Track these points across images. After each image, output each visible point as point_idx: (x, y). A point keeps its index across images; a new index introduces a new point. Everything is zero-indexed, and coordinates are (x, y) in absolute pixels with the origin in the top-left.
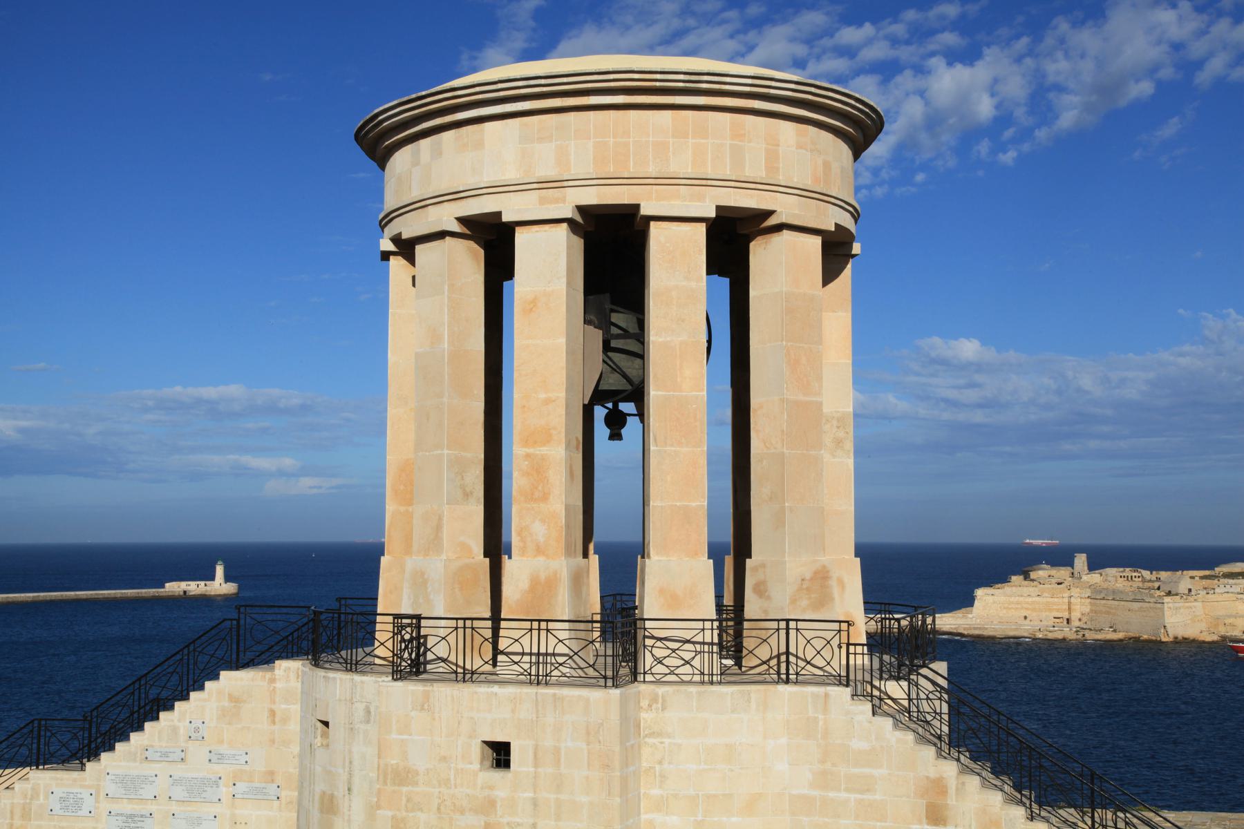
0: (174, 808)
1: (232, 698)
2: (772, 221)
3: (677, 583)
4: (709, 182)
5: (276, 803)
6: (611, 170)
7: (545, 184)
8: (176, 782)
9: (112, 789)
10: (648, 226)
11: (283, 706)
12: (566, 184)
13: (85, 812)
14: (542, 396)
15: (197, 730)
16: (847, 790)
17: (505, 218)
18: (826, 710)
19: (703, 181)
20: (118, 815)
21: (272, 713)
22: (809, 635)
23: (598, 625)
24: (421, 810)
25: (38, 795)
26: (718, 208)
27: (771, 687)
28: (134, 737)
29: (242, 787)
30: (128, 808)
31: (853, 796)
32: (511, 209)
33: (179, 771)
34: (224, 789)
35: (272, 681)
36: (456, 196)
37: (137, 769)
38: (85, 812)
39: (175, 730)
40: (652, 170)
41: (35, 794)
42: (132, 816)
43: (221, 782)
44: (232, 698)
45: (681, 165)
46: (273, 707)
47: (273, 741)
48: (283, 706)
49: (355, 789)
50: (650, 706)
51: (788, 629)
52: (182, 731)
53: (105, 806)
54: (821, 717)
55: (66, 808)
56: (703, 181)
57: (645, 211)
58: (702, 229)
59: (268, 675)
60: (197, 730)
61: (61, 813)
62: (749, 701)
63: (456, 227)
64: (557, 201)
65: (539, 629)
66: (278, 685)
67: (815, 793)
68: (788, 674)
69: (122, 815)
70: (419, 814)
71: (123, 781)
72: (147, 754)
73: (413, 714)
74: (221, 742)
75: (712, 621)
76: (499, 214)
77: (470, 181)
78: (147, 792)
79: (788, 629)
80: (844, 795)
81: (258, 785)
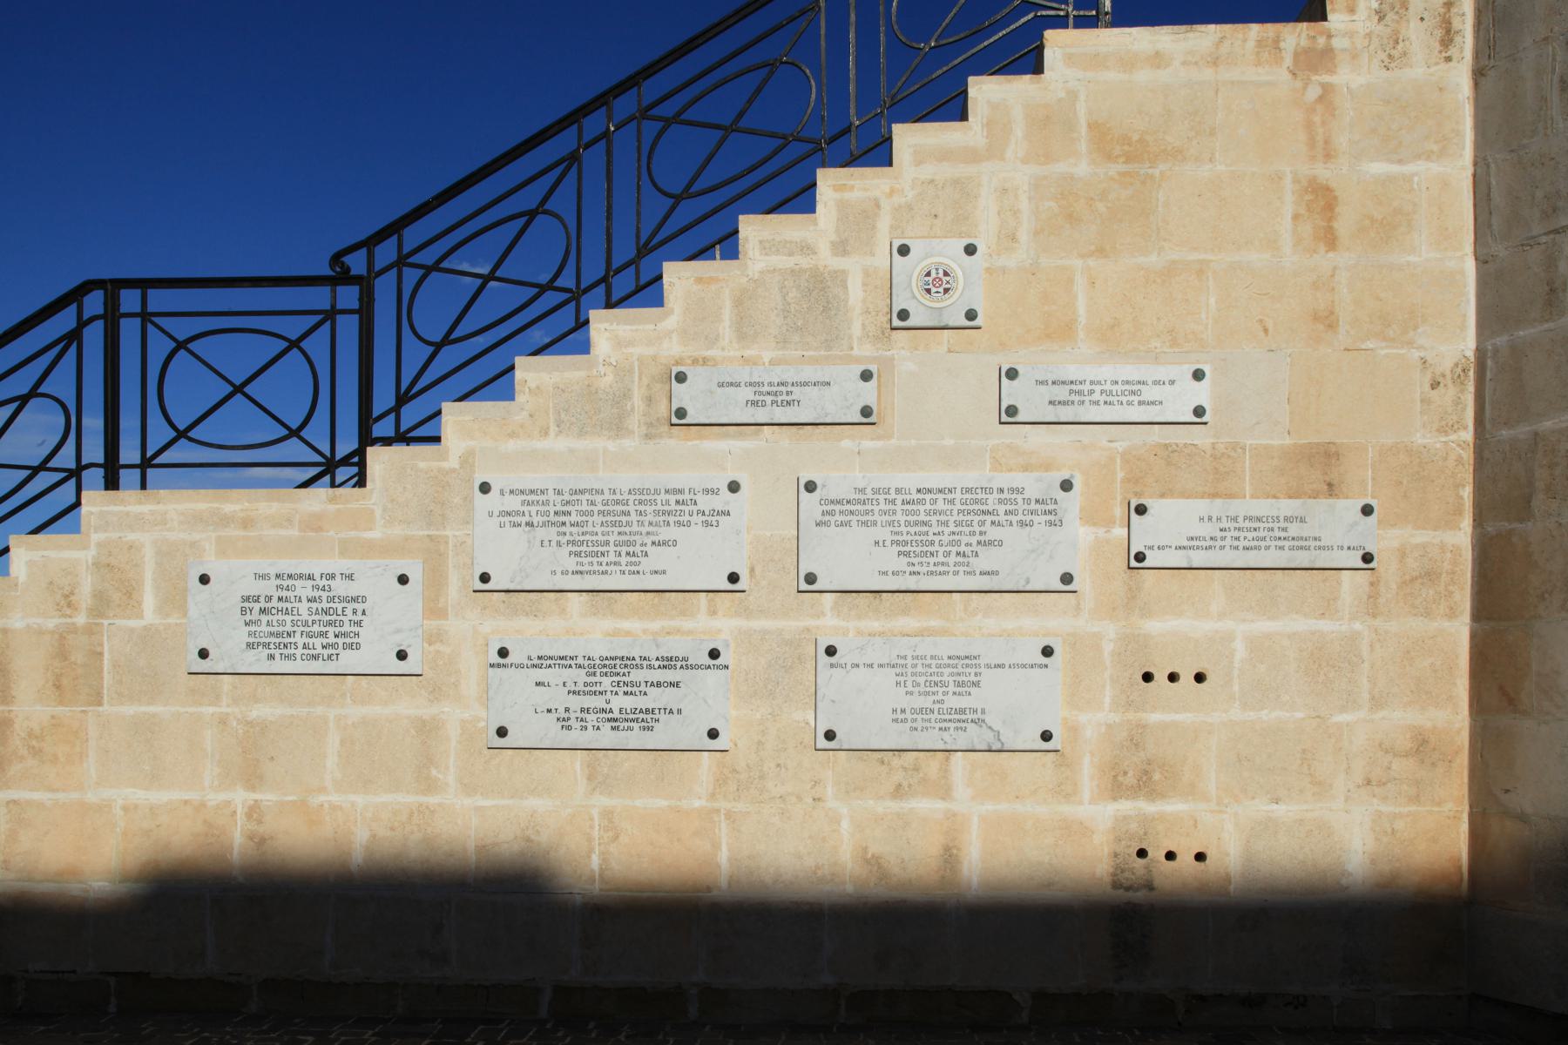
0: (829, 621)
1: (1105, 141)
5: (1351, 585)
8: (849, 510)
9: (508, 553)
11: (1378, 168)
13: (374, 653)
15: (938, 282)
20: (542, 661)
21: (1322, 201)
25: (130, 593)
28: (608, 328)
29: (1173, 523)
30: (594, 632)
33: (845, 466)
34: (1084, 534)
35: (1317, 60)
37: (629, 463)
38: (374, 653)
39: (820, 291)
41: (116, 589)
43: (1070, 504)
44: (1100, 132)
46: (1323, 172)
47: (1327, 320)
48: (1378, 168)
52: (855, 292)
53: (475, 628)
55: (281, 643)
59: (1294, 35)
60: (938, 282)
61: (256, 661)
66: (1345, 77)
69: (564, 661)
71: (557, 514)
72: (683, 395)
74: (1060, 331)
78: (694, 558)
81: (1262, 507)
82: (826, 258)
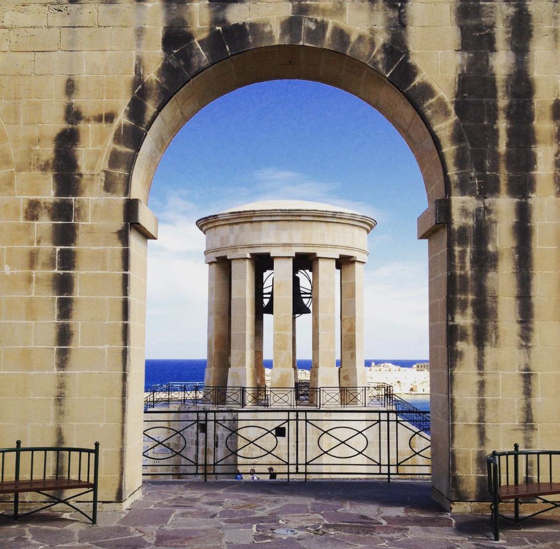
2: (352, 259)
6: (307, 242)
7: (285, 245)
10: (318, 260)
12: (292, 245)
14: (284, 315)
17: (272, 255)
19: (335, 247)
22: (289, 395)
24: (254, 450)
26: (340, 255)
36: (251, 247)
40: (320, 242)
45: (328, 241)
51: (365, 390)
56: (335, 247)
57: (318, 255)
58: (334, 263)
63: (249, 256)
64: (289, 250)
68: (365, 404)
70: (253, 452)
77: (256, 242)
79: (365, 390)
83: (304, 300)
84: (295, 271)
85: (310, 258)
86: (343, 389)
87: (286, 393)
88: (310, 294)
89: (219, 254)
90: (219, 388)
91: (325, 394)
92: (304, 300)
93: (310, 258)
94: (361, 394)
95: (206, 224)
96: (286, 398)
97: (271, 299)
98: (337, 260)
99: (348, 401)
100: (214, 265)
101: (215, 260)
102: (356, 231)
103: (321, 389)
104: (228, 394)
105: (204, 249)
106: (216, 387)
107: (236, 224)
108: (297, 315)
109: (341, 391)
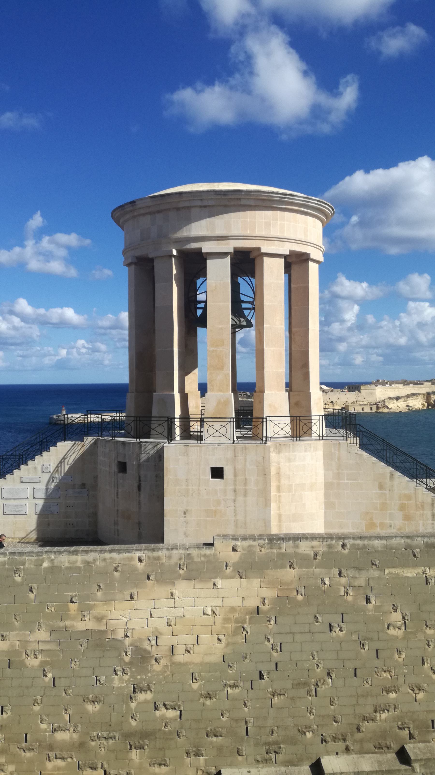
3: (275, 402)
4: (286, 240)
14: (220, 326)
16: (347, 479)
18: (339, 450)
19: (283, 240)
23: (199, 419)
26: (290, 251)
27: (318, 442)
31: (349, 482)
32: (207, 247)
40: (264, 233)
42: (16, 506)
49: (142, 489)
50: (274, 450)
54: (337, 452)
57: (263, 251)
62: (311, 447)
65: (296, 420)
67: (335, 481)
73: (180, 457)
75: (233, 418)
76: (201, 249)
80: (346, 481)
82: (36, 466)
83: (245, 311)
84: (234, 276)
85: (252, 256)
86: (295, 418)
87: (224, 424)
88: (252, 303)
89: (138, 253)
90: (141, 419)
91: (272, 425)
92: (245, 311)
93: (252, 256)
94: (318, 424)
95: (123, 214)
96: (223, 431)
97: (205, 309)
98: (285, 257)
99: (302, 433)
100: (133, 267)
101: (135, 260)
102: (310, 219)
103: (268, 418)
104: (153, 426)
105: (122, 247)
106: (137, 417)
107: (159, 212)
108: (237, 330)
109: (292, 421)
